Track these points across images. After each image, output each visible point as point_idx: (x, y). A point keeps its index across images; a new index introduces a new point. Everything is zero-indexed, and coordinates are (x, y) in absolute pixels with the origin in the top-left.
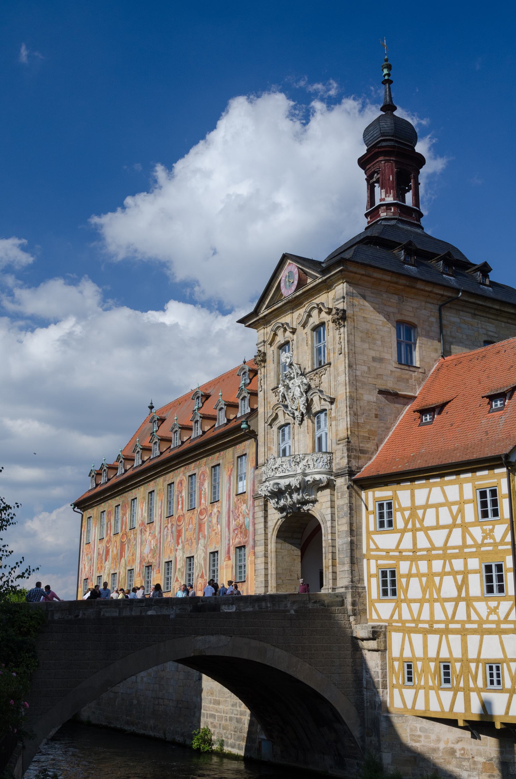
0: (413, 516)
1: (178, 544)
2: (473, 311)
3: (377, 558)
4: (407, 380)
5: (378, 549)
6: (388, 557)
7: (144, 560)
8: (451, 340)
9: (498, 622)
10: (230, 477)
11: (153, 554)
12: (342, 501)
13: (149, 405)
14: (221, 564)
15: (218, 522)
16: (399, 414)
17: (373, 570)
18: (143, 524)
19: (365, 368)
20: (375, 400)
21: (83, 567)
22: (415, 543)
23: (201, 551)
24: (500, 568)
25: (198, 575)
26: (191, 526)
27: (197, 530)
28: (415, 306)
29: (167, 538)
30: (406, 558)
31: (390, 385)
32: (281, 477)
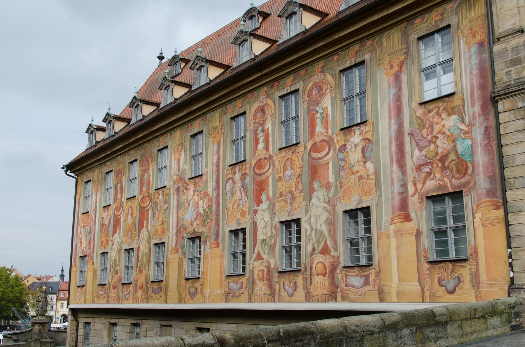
1: (259, 202)
7: (185, 229)
10: (397, 78)
11: (204, 220)
13: (159, 55)
14: (379, 229)
15: (365, 159)
18: (181, 179)
21: (78, 241)
23: (320, 210)
25: (314, 250)
26: (288, 172)
27: (306, 178)
29: (232, 196)
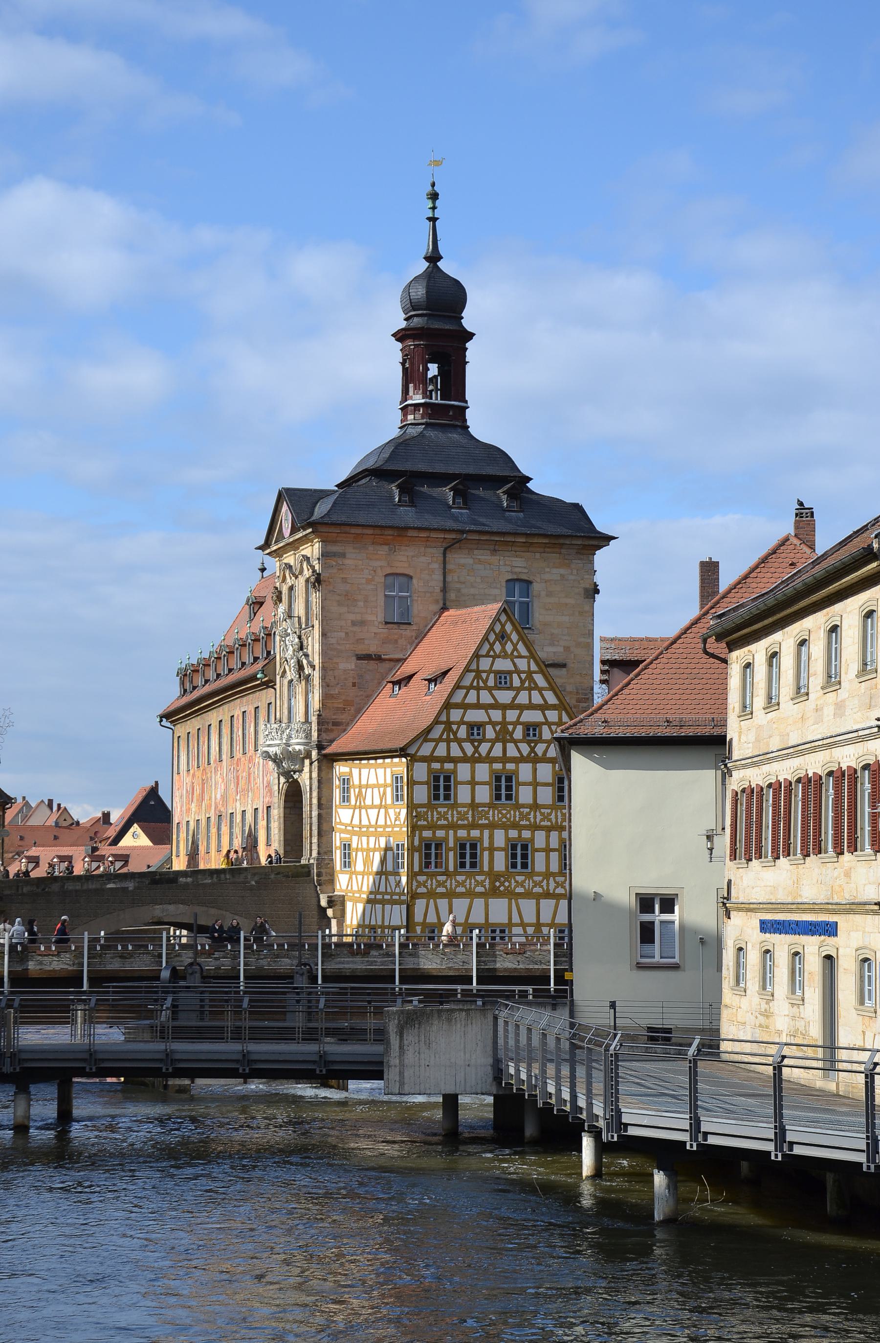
0: (360, 792)
2: (492, 547)
3: (342, 831)
4: (396, 641)
5: (341, 823)
6: (345, 831)
8: (458, 586)
9: (400, 894)
12: (315, 775)
16: (383, 679)
17: (338, 844)
19: (343, 635)
20: (353, 667)
22: (360, 821)
24: (403, 845)
28: (411, 554)
30: (354, 833)
31: (373, 648)
32: (269, 746)
